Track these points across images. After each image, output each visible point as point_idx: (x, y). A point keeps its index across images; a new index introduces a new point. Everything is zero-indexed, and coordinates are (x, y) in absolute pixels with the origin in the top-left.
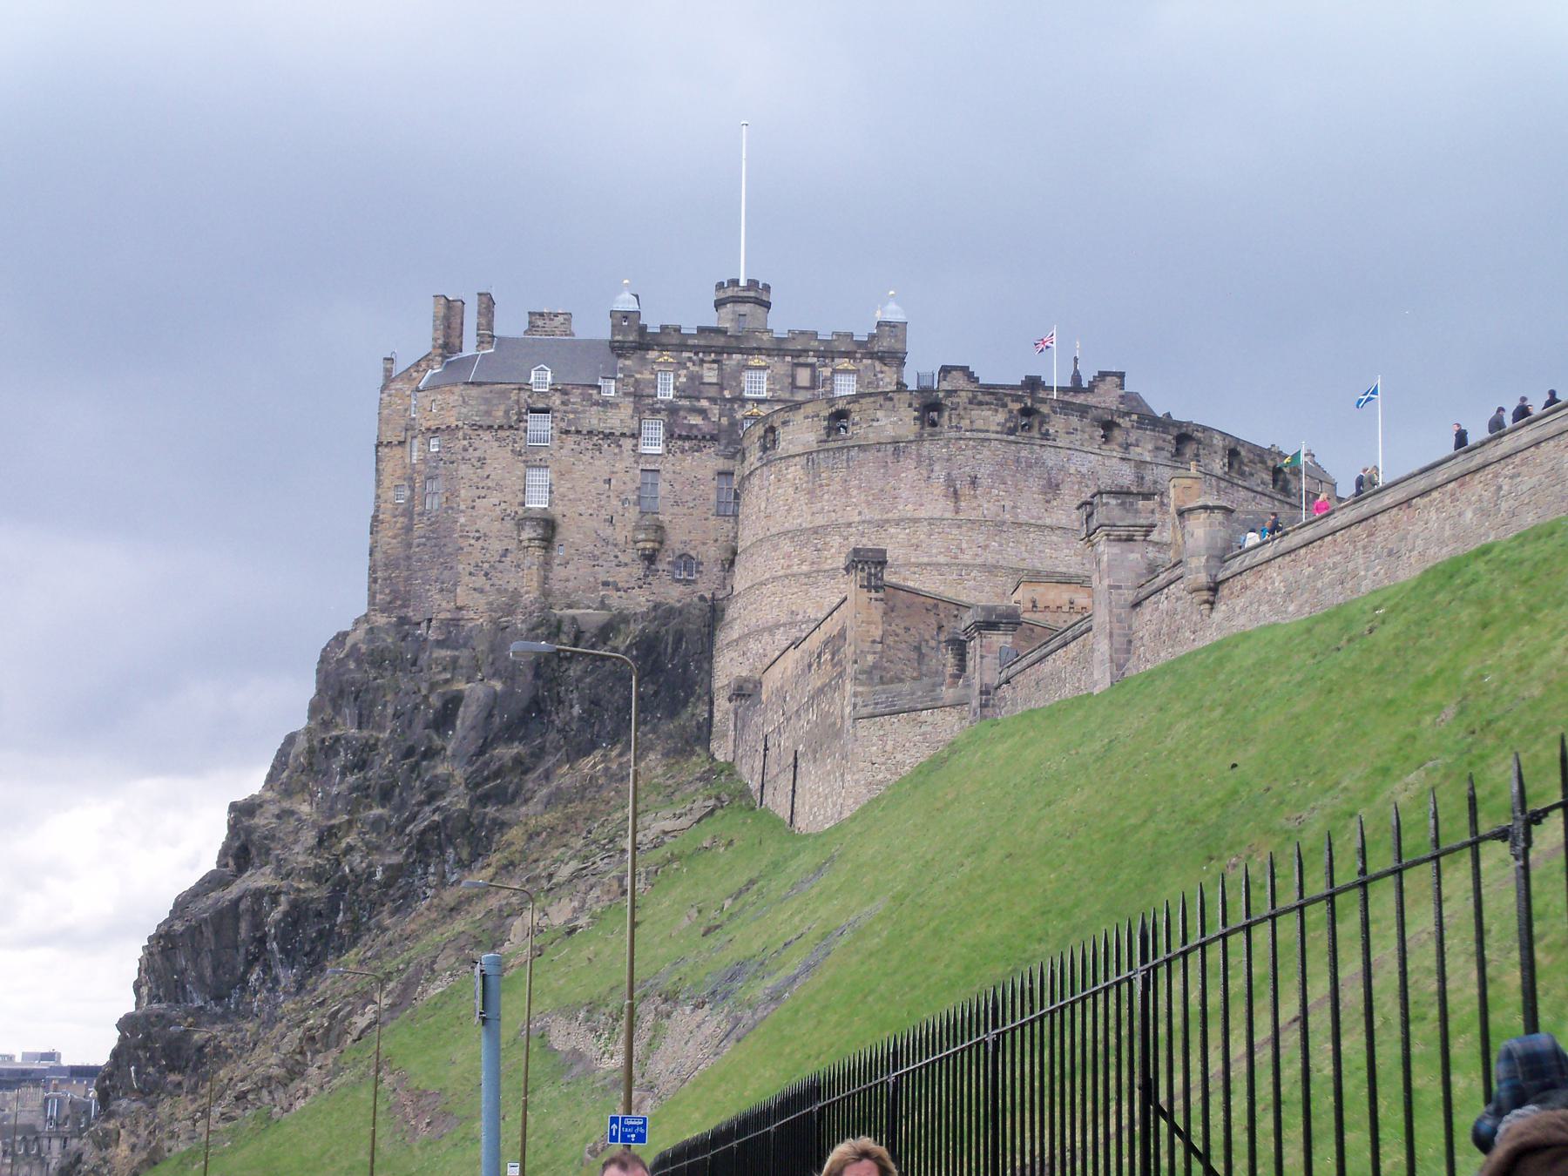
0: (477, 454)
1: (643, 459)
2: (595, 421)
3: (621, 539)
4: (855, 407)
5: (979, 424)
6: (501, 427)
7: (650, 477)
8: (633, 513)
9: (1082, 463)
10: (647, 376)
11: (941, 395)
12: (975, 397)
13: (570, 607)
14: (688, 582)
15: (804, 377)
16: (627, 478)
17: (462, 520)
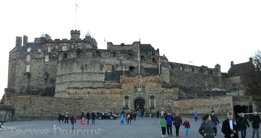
0: (19, 63)
2: (37, 56)
3: (41, 77)
4: (67, 53)
5: (87, 55)
6: (22, 58)
8: (43, 72)
9: (108, 61)
10: (47, 48)
11: (81, 50)
12: (86, 50)
13: (32, 89)
14: (53, 83)
15: (73, 47)
16: (43, 66)
17: (16, 74)
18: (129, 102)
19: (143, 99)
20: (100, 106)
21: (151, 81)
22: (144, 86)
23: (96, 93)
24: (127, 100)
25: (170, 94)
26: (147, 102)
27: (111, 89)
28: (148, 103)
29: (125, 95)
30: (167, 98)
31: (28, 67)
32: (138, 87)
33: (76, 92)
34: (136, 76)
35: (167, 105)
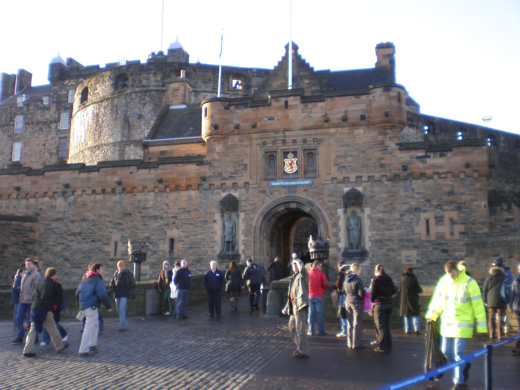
1: (60, 133)
2: (39, 117)
5: (145, 82)
6: (4, 126)
7: (63, 141)
10: (64, 92)
18: (242, 227)
19: (307, 209)
20: (110, 249)
21: (345, 119)
22: (310, 144)
23: (94, 192)
24: (234, 215)
25: (448, 183)
26: (329, 222)
27: (161, 167)
28: (332, 230)
29: (224, 195)
30: (429, 201)
31: (18, 147)
32: (285, 154)
33: (18, 189)
34: (274, 104)
35: (433, 237)
